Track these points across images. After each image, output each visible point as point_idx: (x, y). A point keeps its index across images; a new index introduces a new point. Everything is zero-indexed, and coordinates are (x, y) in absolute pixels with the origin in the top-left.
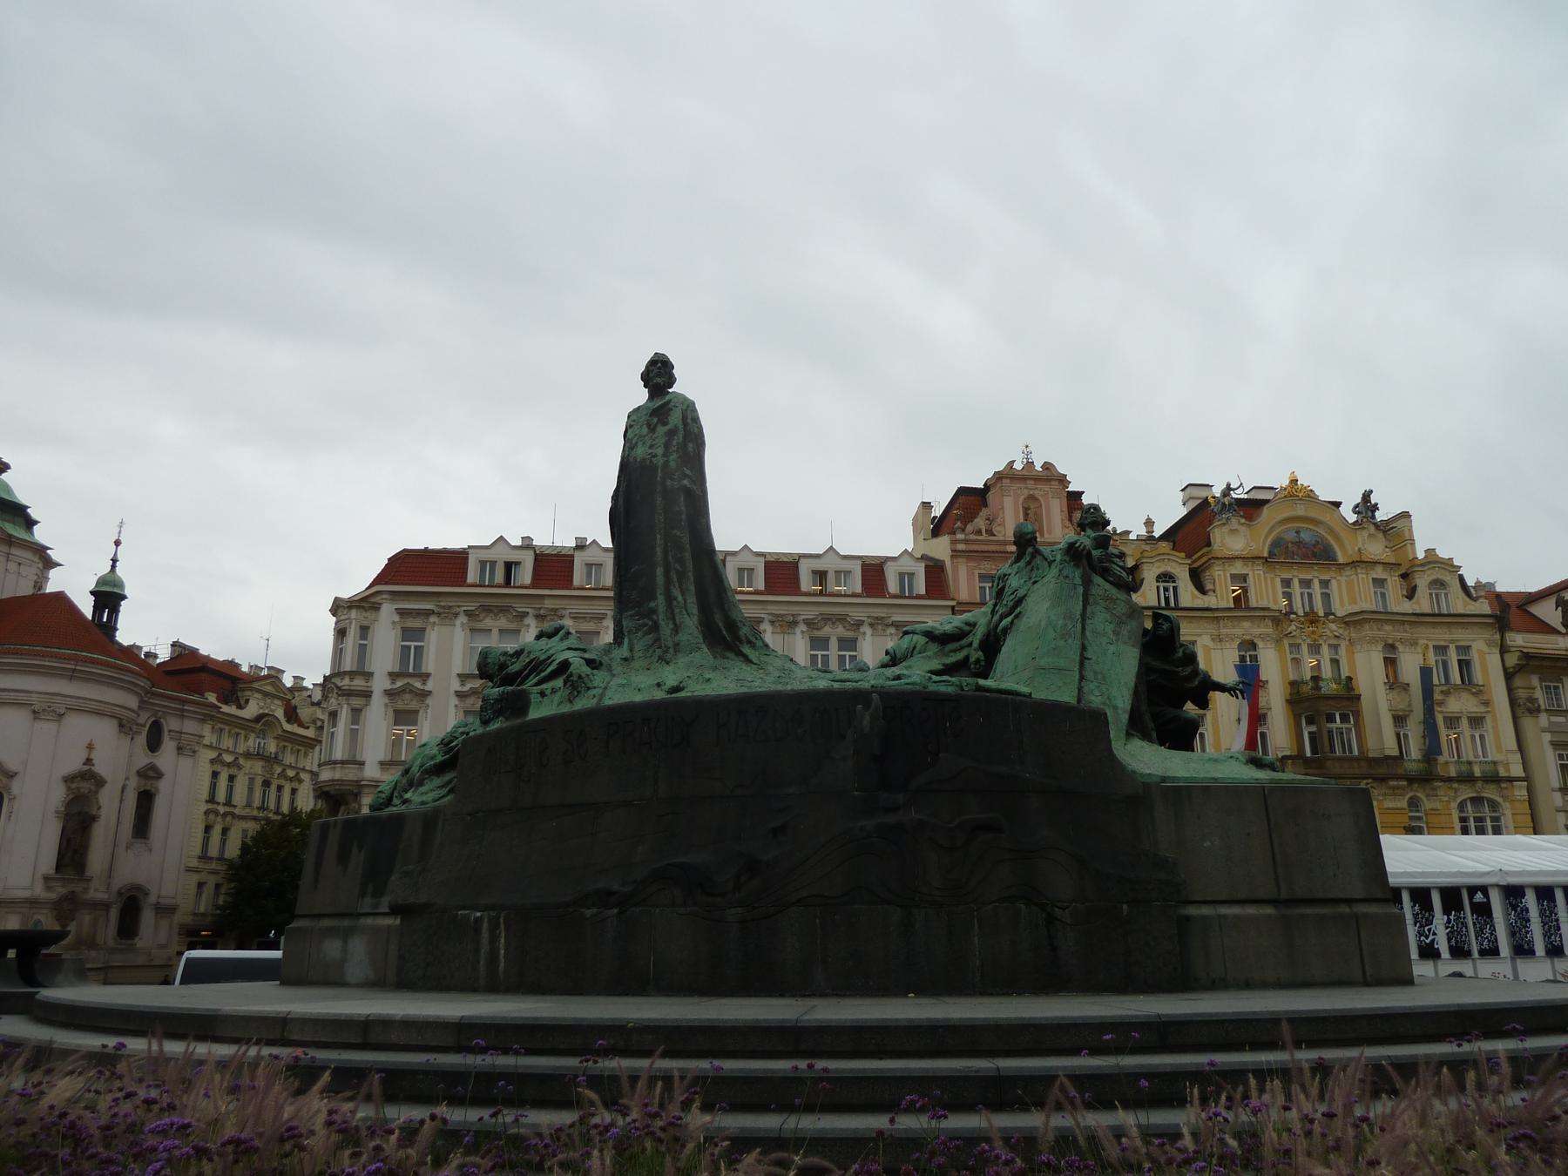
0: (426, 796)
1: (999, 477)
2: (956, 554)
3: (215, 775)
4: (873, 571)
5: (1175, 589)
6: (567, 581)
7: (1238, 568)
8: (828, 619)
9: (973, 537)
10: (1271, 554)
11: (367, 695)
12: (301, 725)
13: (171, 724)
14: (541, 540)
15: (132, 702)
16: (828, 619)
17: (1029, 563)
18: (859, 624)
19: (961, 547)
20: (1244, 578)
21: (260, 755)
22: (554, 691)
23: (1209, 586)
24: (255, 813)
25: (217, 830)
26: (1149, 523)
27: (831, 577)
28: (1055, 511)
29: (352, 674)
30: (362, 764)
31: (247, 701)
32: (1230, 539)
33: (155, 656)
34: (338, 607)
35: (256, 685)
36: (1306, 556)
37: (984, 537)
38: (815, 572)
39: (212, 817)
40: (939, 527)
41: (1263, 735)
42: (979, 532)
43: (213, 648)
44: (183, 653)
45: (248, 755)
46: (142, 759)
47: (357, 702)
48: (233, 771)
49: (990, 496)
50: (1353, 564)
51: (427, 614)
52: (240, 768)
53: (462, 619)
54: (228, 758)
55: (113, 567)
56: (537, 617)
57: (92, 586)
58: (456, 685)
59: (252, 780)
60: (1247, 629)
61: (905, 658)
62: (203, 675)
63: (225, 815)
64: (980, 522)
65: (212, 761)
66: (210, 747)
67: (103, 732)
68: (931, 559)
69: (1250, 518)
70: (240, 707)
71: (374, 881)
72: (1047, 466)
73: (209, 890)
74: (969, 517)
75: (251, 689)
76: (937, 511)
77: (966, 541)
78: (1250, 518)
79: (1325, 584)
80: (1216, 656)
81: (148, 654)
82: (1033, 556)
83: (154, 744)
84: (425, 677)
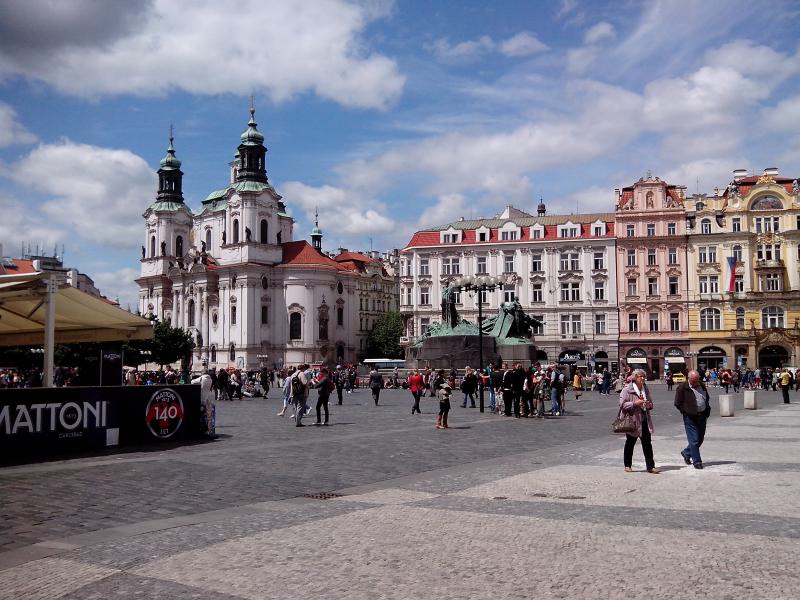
0: (421, 344)
1: (637, 185)
3: (361, 300)
13: (344, 283)
15: (333, 278)
21: (375, 290)
25: (364, 320)
27: (569, 232)
38: (563, 230)
42: (627, 208)
46: (338, 296)
50: (789, 211)
58: (440, 279)
64: (628, 204)
67: (326, 290)
71: (415, 355)
79: (776, 219)
83: (340, 291)
84: (430, 277)
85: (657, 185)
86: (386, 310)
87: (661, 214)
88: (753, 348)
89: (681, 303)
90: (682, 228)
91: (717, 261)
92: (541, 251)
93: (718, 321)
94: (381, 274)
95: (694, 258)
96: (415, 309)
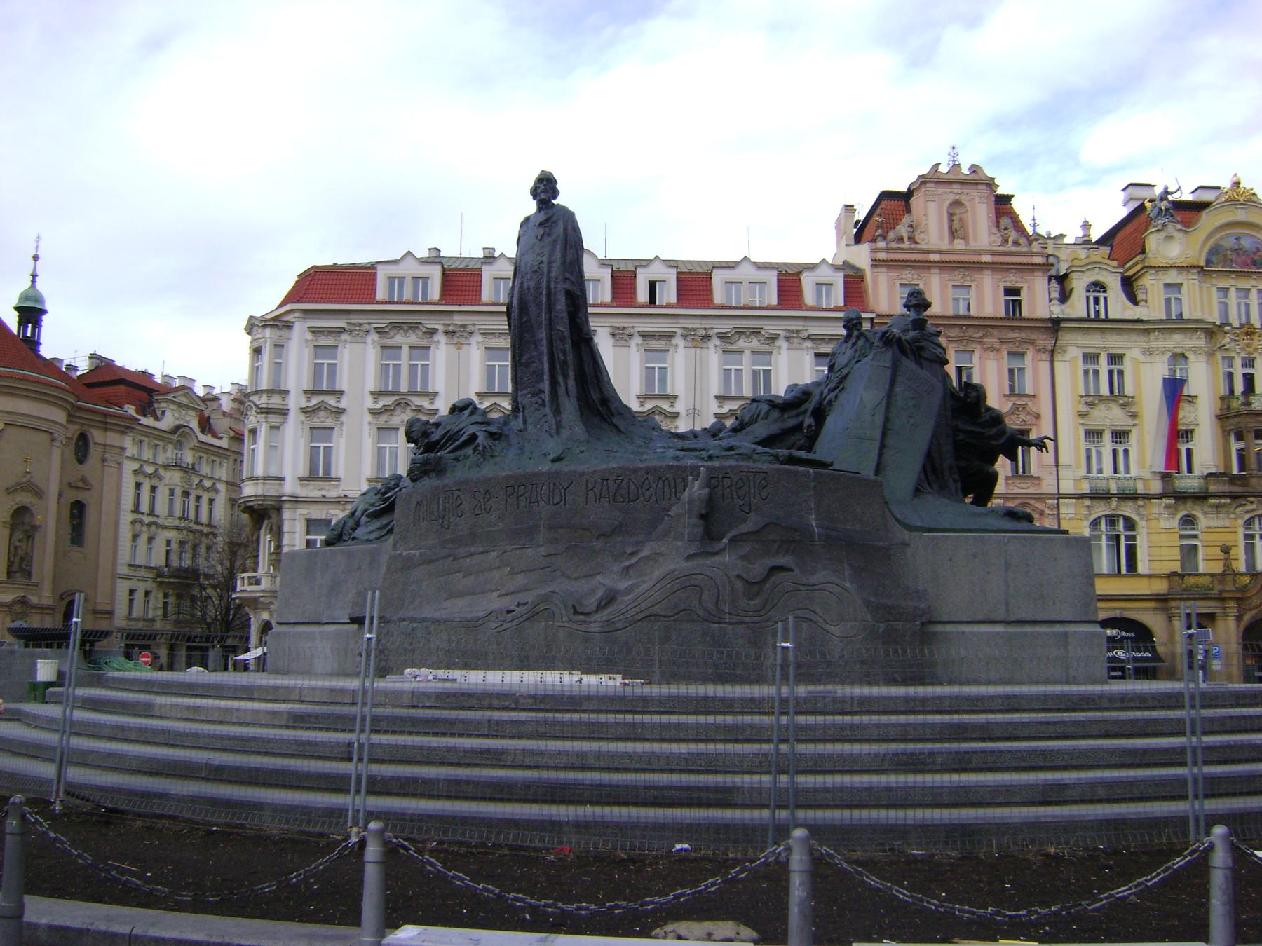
1: (923, 181)
2: (876, 263)
3: (138, 485)
4: (789, 282)
5: (1106, 299)
6: (475, 297)
7: (1172, 277)
8: (740, 332)
9: (894, 245)
10: (1208, 262)
11: (284, 412)
12: (215, 435)
13: (97, 436)
14: (450, 251)
15: (60, 416)
16: (740, 332)
17: (854, 344)
18: (773, 338)
19: (882, 256)
20: (1178, 286)
21: (177, 466)
22: (466, 457)
23: (1140, 296)
24: (177, 523)
25: (144, 538)
26: (1086, 226)
28: (980, 215)
29: (270, 392)
30: (282, 479)
31: (164, 412)
32: (1168, 246)
33: (75, 369)
34: (253, 325)
35: (170, 397)
36: (1247, 265)
37: (906, 245)
39: (138, 526)
40: (861, 233)
41: (1189, 452)
42: (901, 240)
43: (129, 359)
44: (102, 366)
45: (167, 467)
47: (275, 419)
48: (155, 482)
49: (913, 200)
51: (339, 331)
52: (161, 478)
53: (374, 336)
54: (150, 470)
55: (34, 282)
56: (447, 333)
57: (15, 302)
58: (369, 402)
59: (172, 492)
60: (1177, 341)
61: (750, 423)
62: (122, 388)
63: (149, 525)
64: (902, 230)
65: (136, 472)
66: (132, 458)
68: (853, 267)
69: (1187, 225)
70: (157, 419)
72: (975, 169)
73: (139, 597)
74: (891, 223)
75: (168, 401)
76: (861, 215)
77: (887, 250)
78: (1187, 225)
80: (1145, 369)
81: (70, 367)
82: (858, 338)
84: (339, 394)
85: (975, 184)
86: (204, 518)
87: (986, 258)
88: (1231, 623)
89: (1041, 498)
90: (1039, 300)
91: (1129, 390)
92: (670, 336)
93: (1131, 551)
94: (194, 424)
95: (1069, 370)
96: (290, 487)
